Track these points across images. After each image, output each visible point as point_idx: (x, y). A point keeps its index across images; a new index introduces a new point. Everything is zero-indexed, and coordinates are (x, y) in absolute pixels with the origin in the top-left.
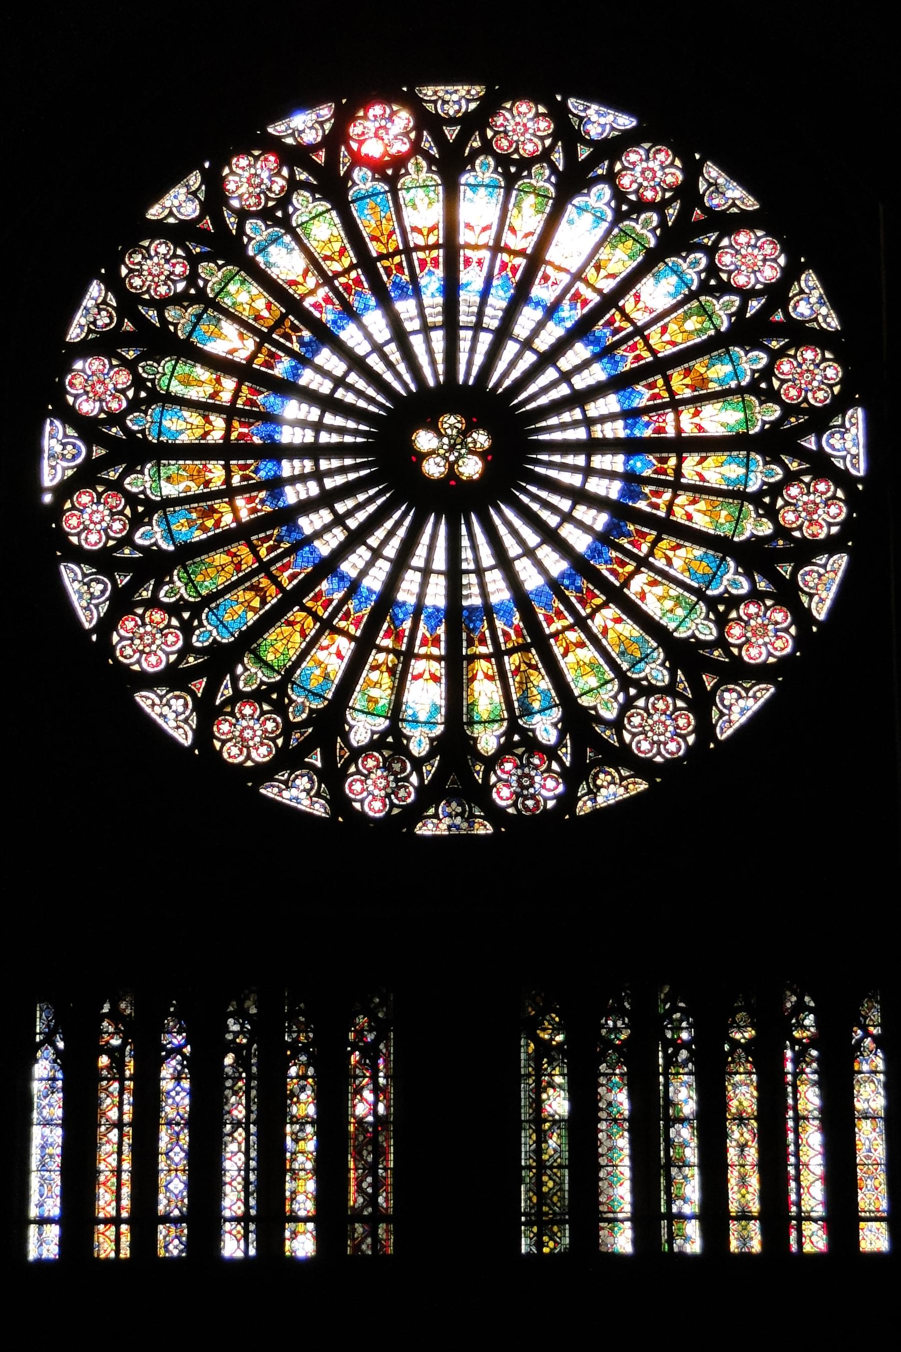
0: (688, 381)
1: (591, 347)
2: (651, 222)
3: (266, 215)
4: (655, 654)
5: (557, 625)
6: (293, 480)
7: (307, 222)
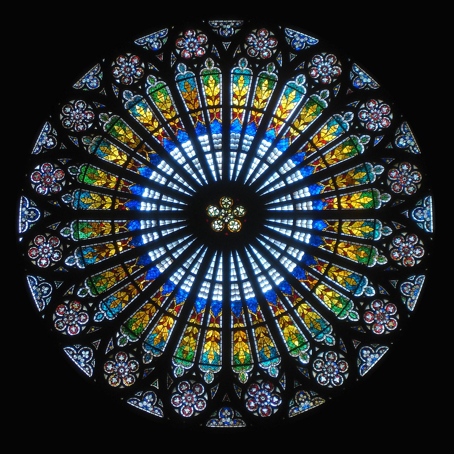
0: (344, 181)
1: (296, 162)
2: (326, 95)
3: (134, 88)
4: (328, 329)
5: (279, 312)
6: (146, 231)
7: (154, 92)
